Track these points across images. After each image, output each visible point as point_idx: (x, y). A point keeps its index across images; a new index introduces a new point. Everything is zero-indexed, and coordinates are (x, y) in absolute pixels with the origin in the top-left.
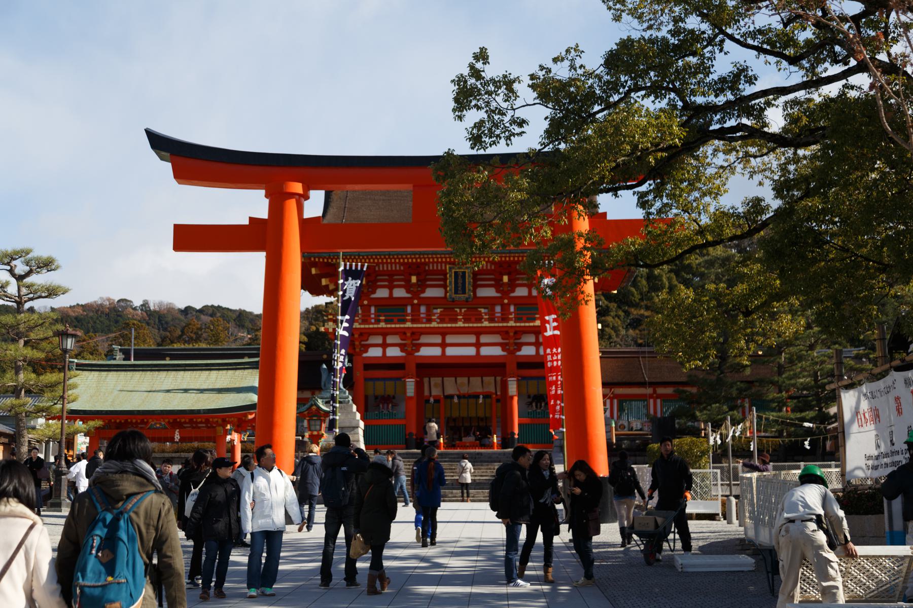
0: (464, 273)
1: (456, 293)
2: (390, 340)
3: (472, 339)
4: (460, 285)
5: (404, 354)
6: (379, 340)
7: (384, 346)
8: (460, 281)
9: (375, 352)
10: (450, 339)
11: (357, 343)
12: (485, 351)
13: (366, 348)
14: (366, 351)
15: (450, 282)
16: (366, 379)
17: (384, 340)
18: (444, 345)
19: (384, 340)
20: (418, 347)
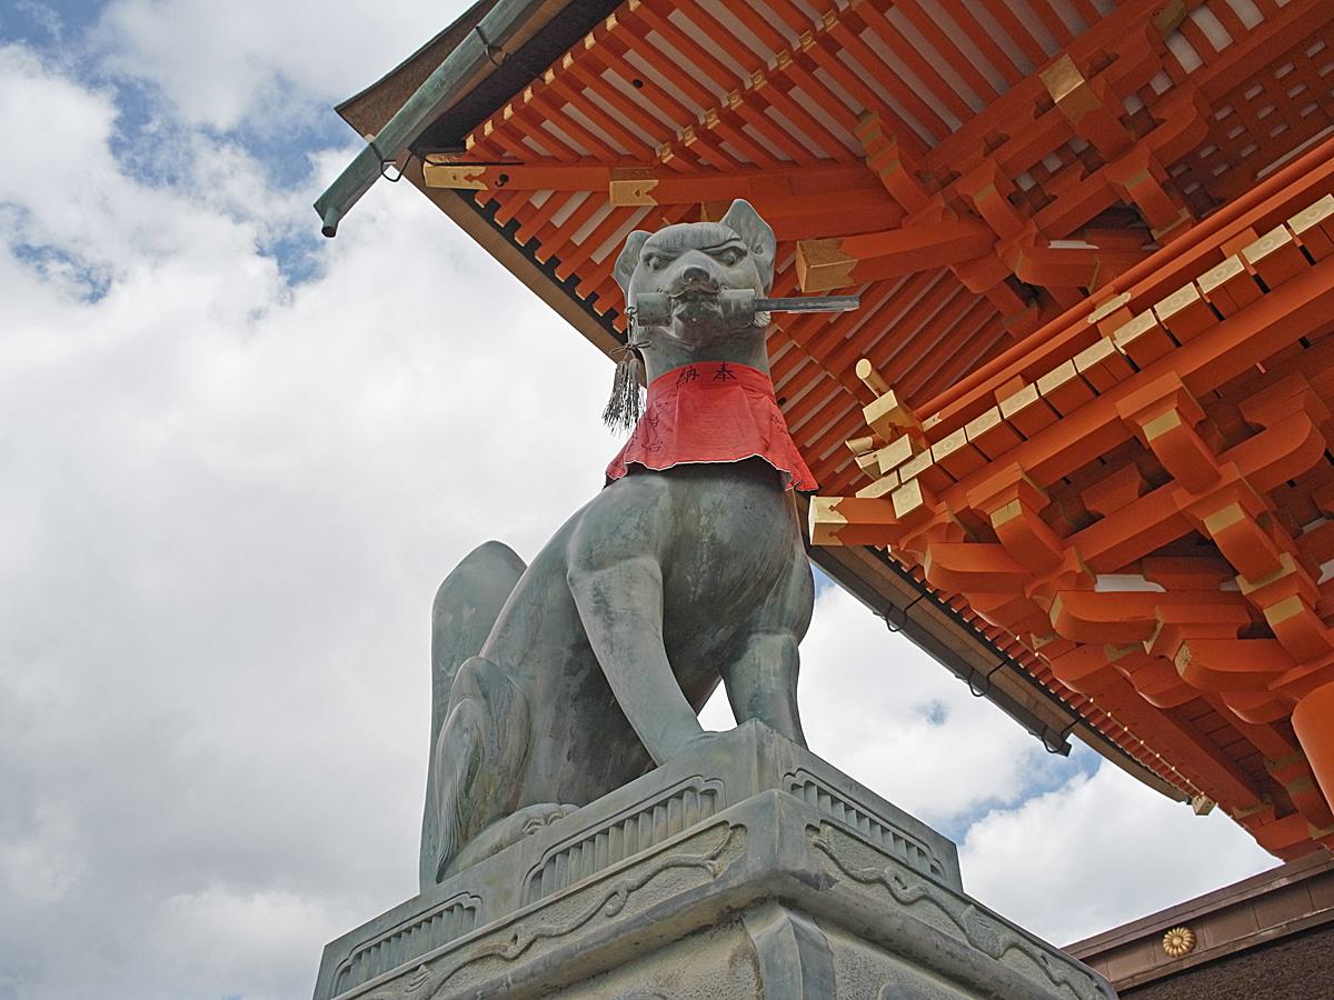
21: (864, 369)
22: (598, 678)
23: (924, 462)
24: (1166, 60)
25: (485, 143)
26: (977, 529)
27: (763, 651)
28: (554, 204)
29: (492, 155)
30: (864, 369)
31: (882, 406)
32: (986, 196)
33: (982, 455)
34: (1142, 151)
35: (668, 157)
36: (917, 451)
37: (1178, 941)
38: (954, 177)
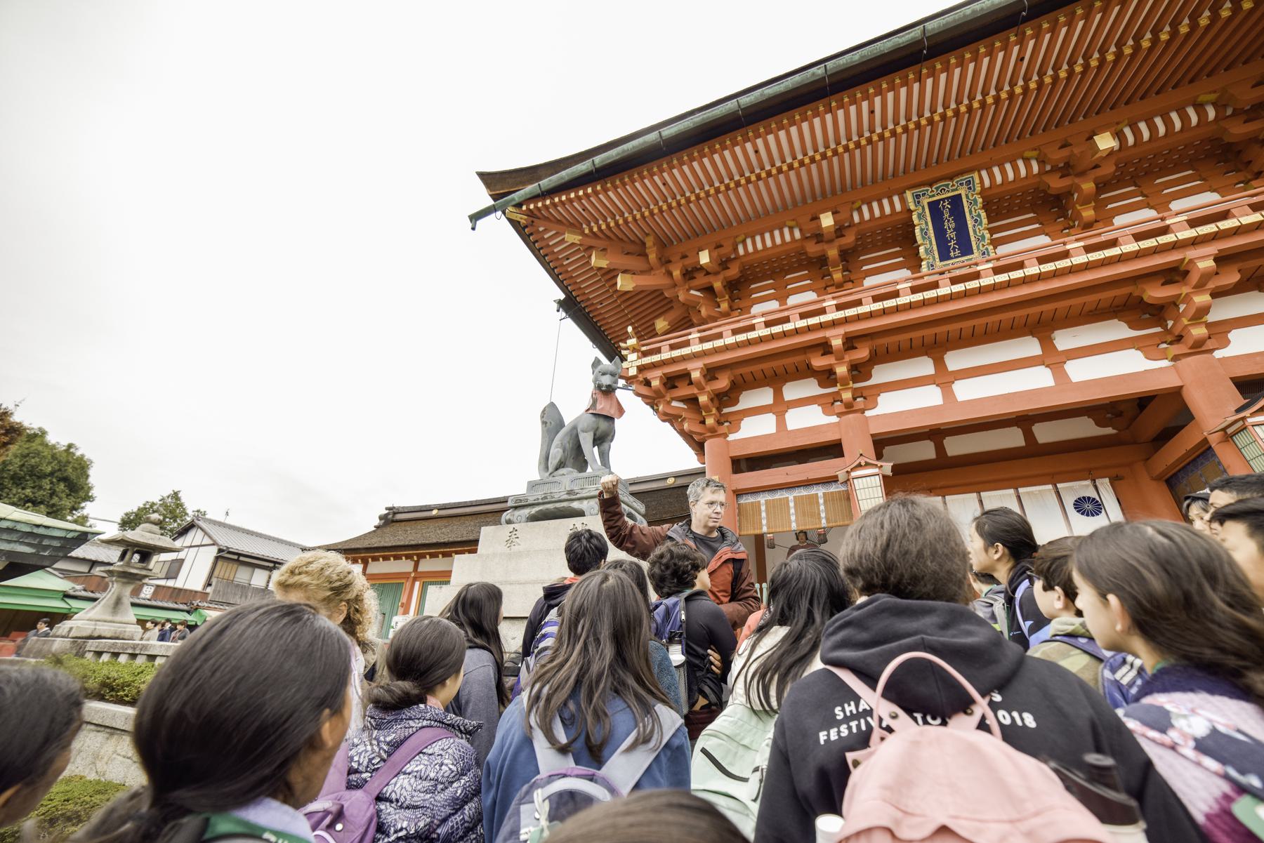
0: (956, 201)
1: (944, 256)
2: (792, 391)
3: (1029, 347)
4: (951, 234)
5: (834, 419)
6: (764, 396)
7: (780, 407)
8: (950, 225)
9: (755, 429)
10: (956, 360)
11: (703, 399)
12: (1082, 371)
13: (734, 421)
14: (737, 429)
15: (925, 233)
16: (739, 493)
17: (778, 394)
18: (944, 379)
19: (778, 394)
20: (870, 396)
21: (630, 329)
22: (579, 446)
23: (639, 363)
24: (736, 250)
25: (528, 209)
26: (647, 383)
27: (605, 445)
28: (546, 231)
29: (530, 213)
30: (630, 329)
31: (632, 342)
32: (677, 273)
33: (654, 366)
34: (721, 276)
35: (587, 231)
36: (639, 358)
37: (671, 481)
38: (670, 262)
